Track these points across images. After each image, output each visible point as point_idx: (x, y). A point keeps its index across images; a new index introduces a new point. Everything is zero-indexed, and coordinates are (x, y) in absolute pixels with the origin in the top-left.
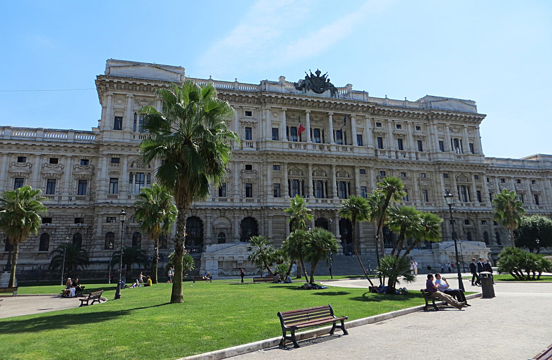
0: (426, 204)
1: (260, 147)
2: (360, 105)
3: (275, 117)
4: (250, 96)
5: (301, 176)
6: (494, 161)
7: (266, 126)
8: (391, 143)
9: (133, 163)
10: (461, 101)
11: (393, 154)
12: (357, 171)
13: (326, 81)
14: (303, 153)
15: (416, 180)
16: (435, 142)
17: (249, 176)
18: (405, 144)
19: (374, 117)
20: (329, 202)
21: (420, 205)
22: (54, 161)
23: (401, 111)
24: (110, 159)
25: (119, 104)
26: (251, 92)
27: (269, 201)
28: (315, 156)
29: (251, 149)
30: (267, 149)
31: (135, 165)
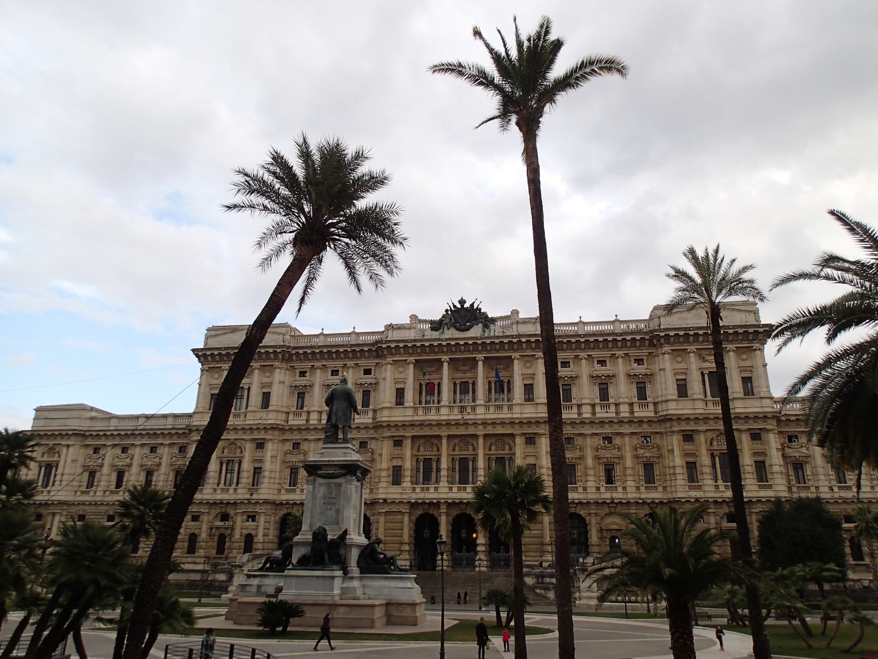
2: (524, 340)
12: (519, 441)
15: (628, 448)
16: (666, 382)
25: (216, 379)
28: (448, 424)
31: (226, 450)
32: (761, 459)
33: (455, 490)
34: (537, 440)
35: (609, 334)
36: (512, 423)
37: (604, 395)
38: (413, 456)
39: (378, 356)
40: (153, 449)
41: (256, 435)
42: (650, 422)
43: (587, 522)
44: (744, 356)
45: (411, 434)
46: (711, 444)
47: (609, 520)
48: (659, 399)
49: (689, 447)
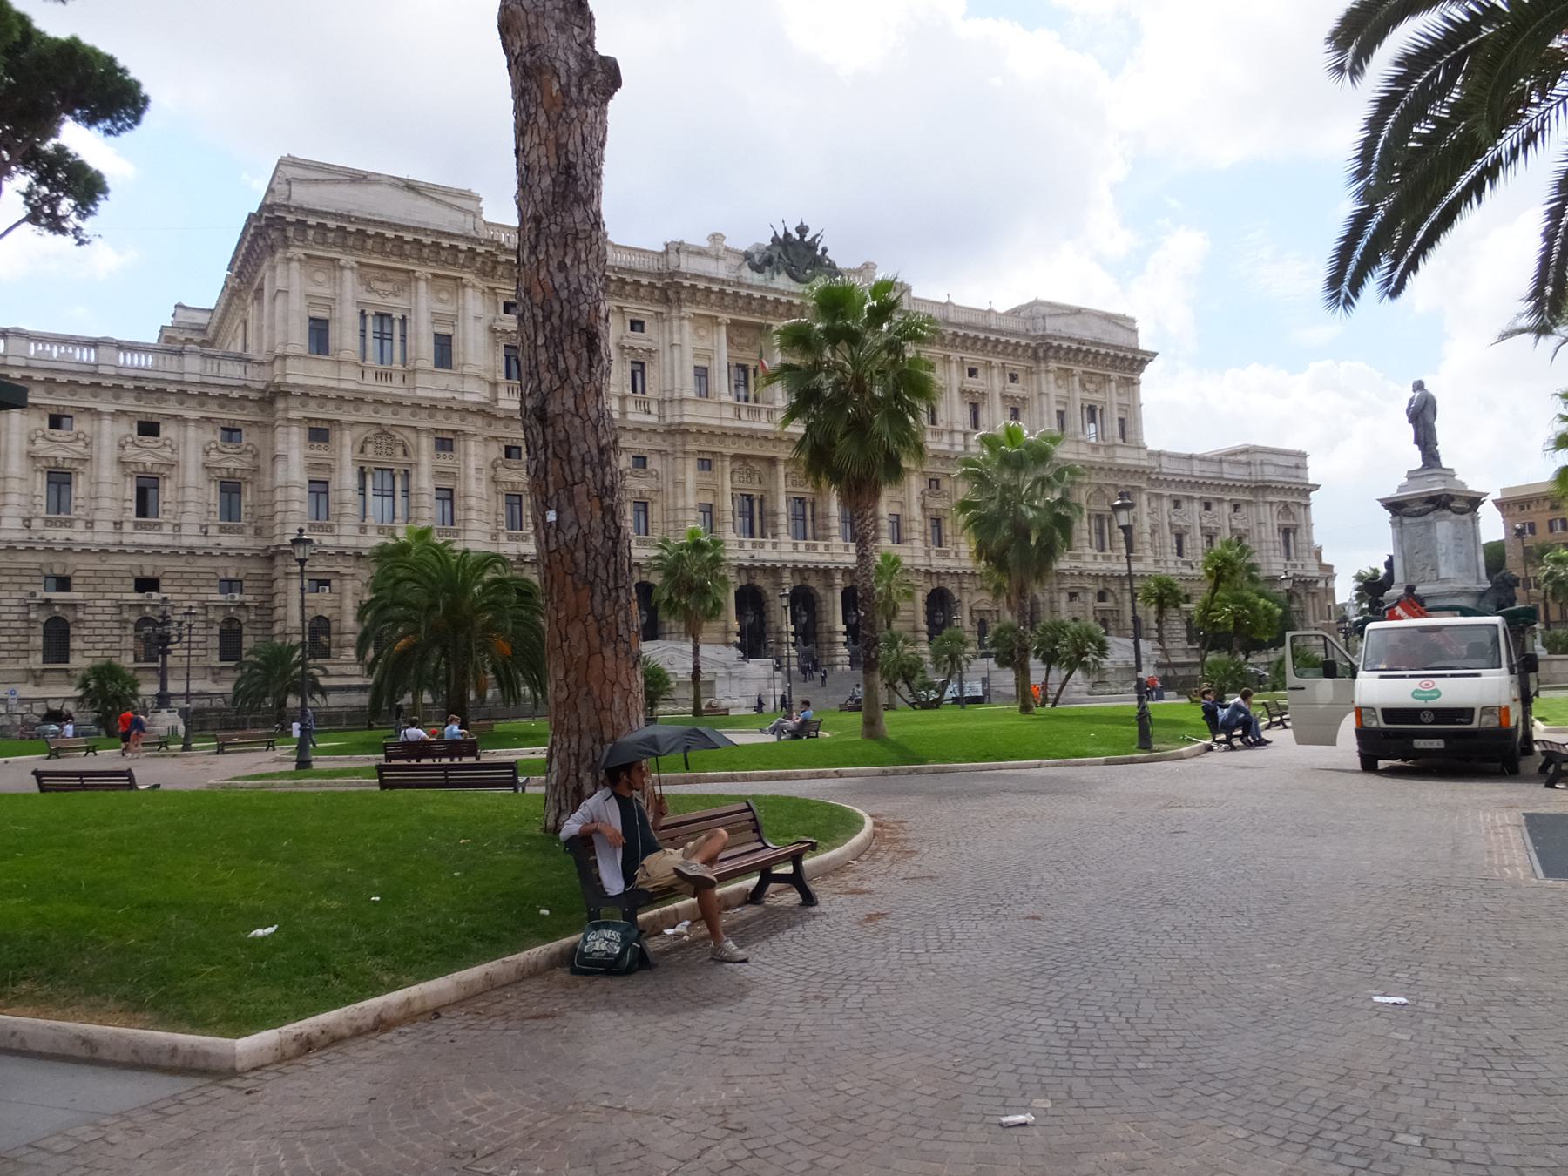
1: (668, 413)
3: (701, 338)
4: (645, 281)
5: (758, 486)
7: (682, 361)
9: (365, 441)
11: (959, 438)
13: (819, 253)
18: (983, 416)
22: (149, 429)
23: (982, 336)
24: (305, 432)
26: (648, 274)
30: (686, 419)
31: (370, 447)
33: (802, 547)
40: (149, 429)
41: (441, 422)
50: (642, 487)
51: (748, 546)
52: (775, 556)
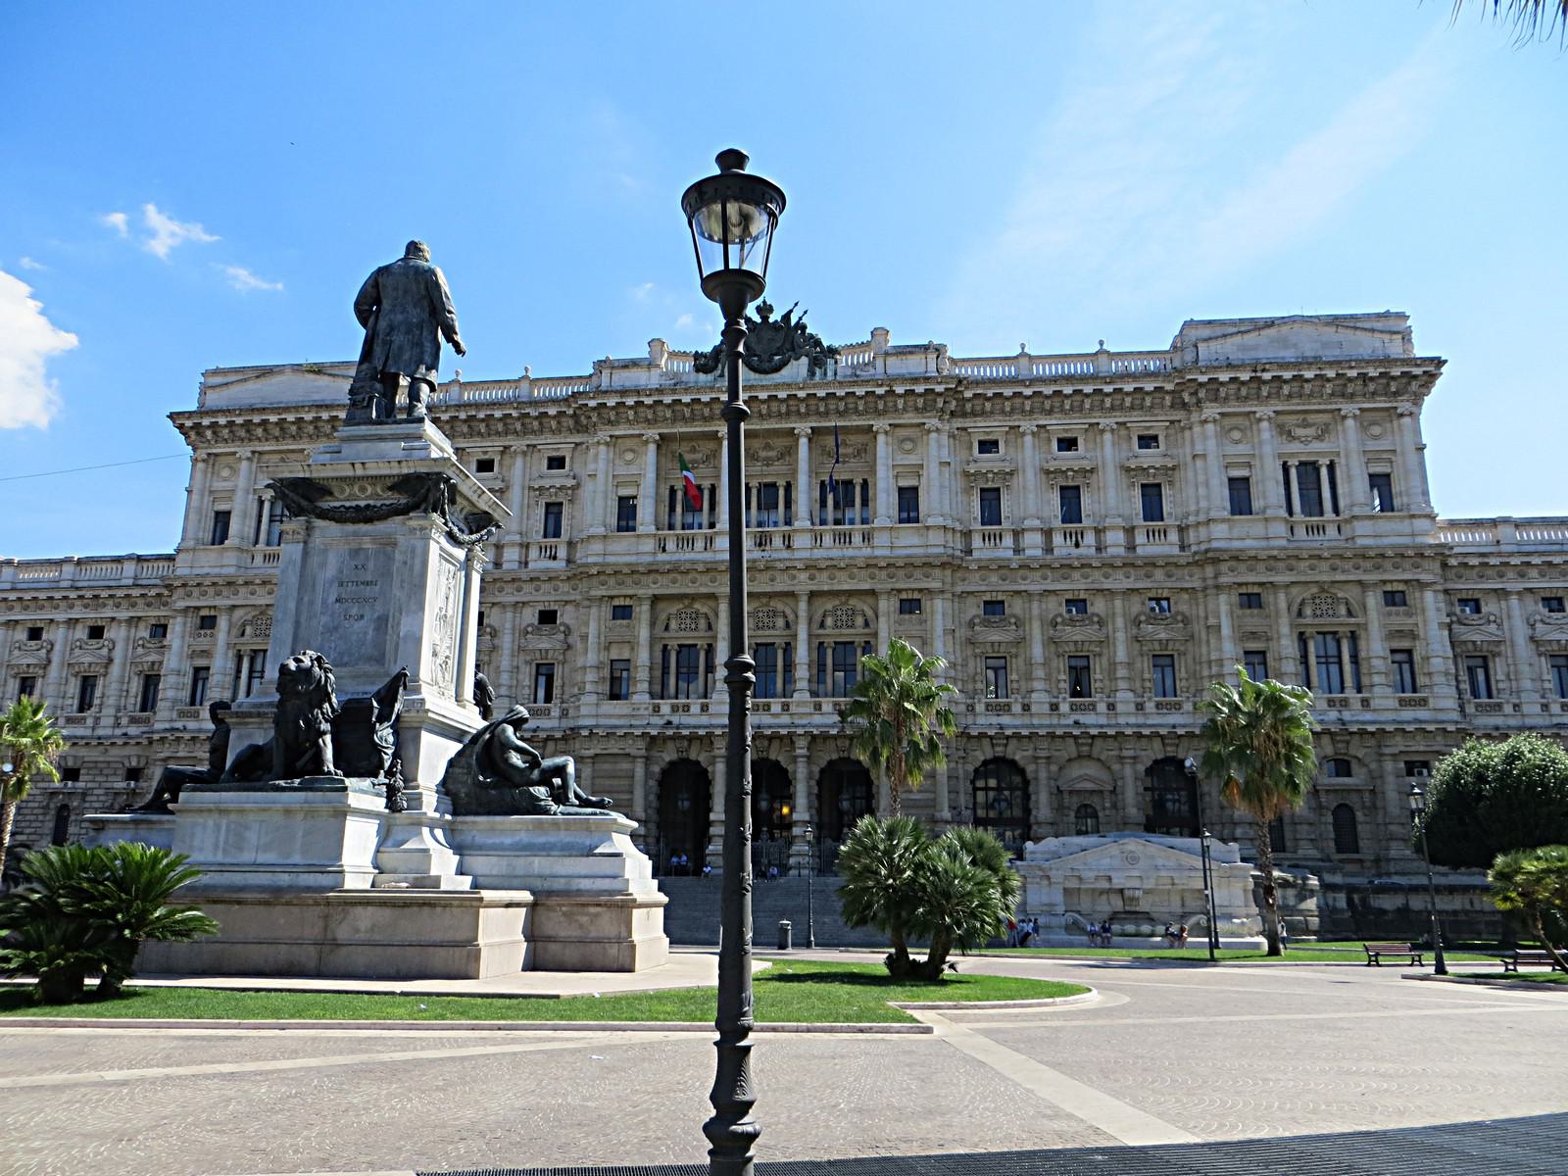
0: (1158, 705)
2: (900, 390)
4: (552, 411)
6: (1505, 532)
8: (1031, 502)
10: (1335, 321)
12: (887, 605)
14: (694, 562)
15: (1120, 622)
16: (1207, 484)
17: (546, 643)
19: (968, 423)
20: (776, 708)
21: (1537, 709)
27: (584, 711)
29: (552, 564)
31: (249, 630)
32: (1405, 644)
34: (926, 604)
35: (1084, 378)
36: (870, 565)
37: (1071, 509)
38: (653, 640)
39: (580, 428)
42: (1170, 565)
43: (1030, 775)
44: (1376, 430)
45: (650, 592)
46: (1300, 614)
47: (1076, 771)
48: (1192, 519)
49: (1253, 620)
50: (544, 645)
51: (665, 709)
52: (704, 720)
